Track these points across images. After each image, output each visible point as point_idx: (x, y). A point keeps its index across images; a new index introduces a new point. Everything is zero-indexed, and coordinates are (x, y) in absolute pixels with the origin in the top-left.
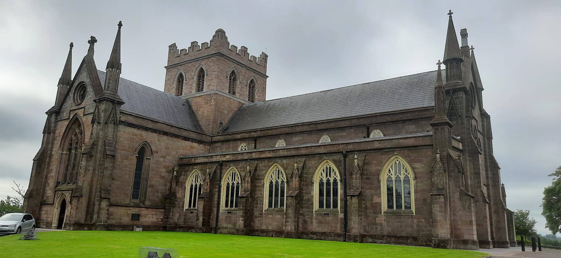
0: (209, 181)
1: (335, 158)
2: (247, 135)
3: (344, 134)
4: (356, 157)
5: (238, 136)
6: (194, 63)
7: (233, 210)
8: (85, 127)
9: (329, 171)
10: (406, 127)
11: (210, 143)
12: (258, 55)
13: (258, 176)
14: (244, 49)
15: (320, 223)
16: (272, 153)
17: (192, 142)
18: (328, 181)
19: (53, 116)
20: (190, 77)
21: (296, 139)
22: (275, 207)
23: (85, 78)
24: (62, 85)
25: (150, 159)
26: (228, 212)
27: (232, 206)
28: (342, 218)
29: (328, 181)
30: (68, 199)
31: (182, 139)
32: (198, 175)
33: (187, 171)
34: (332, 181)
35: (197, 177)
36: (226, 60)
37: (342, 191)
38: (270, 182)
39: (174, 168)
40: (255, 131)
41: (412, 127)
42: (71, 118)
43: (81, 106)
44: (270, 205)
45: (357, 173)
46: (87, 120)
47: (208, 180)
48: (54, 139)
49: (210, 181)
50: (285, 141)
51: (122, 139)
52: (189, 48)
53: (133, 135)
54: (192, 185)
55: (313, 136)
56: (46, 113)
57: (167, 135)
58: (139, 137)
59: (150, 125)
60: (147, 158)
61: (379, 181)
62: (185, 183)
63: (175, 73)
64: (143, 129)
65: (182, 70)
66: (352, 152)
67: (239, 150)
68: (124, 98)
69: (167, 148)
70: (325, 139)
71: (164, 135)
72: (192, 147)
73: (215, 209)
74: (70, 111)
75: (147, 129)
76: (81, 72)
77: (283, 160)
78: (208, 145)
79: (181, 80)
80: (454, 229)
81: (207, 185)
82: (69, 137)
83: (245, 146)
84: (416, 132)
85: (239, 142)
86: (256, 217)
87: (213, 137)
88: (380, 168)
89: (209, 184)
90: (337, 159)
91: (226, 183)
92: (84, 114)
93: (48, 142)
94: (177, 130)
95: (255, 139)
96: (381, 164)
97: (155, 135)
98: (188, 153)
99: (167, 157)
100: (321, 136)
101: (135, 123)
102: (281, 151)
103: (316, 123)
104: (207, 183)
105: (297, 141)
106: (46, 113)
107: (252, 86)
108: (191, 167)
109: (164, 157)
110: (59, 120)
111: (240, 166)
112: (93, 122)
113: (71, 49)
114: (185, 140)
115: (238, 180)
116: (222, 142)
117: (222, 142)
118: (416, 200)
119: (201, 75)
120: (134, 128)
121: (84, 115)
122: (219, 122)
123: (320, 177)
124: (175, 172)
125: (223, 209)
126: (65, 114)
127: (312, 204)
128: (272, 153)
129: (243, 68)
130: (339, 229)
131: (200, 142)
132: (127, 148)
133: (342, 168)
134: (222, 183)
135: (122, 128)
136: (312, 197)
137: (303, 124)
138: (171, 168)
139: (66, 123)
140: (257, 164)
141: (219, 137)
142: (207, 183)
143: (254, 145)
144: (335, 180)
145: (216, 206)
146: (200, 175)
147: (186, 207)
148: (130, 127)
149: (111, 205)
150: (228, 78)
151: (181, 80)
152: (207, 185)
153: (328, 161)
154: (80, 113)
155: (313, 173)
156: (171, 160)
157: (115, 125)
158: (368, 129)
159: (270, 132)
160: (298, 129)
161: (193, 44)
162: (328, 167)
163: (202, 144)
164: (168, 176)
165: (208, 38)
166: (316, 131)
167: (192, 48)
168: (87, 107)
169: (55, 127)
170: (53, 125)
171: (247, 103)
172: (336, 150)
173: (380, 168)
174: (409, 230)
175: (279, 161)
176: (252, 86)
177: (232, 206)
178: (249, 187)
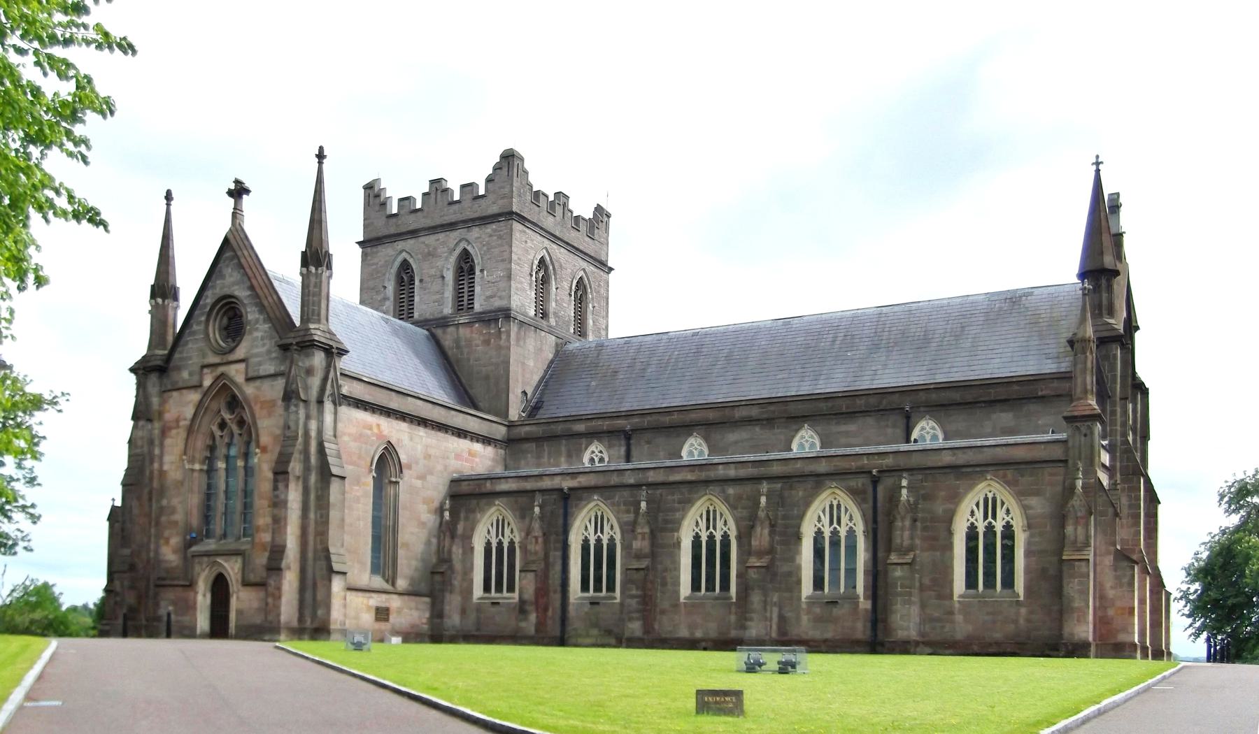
0: (541, 534)
1: (853, 483)
2: (605, 425)
3: (851, 427)
5: (580, 427)
6: (441, 236)
7: (605, 598)
8: (257, 408)
9: (834, 514)
10: (994, 416)
11: (505, 443)
12: (589, 214)
13: (666, 521)
15: (818, 620)
16: (697, 472)
17: (472, 440)
20: (433, 272)
22: (707, 589)
23: (231, 283)
24: (159, 300)
25: (399, 483)
26: (592, 603)
27: (598, 588)
28: (866, 610)
31: (453, 434)
32: (503, 520)
33: (473, 511)
34: (718, 538)
35: (500, 525)
36: (528, 231)
37: (869, 555)
38: (583, 541)
40: (629, 415)
41: (1005, 417)
43: (232, 357)
44: (696, 586)
45: (903, 519)
47: (537, 531)
49: (544, 534)
50: (707, 439)
51: (346, 438)
52: (424, 194)
53: (365, 427)
54: (489, 544)
55: (776, 431)
57: (426, 426)
58: (375, 430)
59: (395, 403)
60: (391, 482)
61: (950, 533)
64: (381, 414)
66: (896, 471)
68: (346, 341)
69: (428, 456)
70: (806, 442)
71: (419, 425)
72: (471, 453)
74: (203, 367)
75: (388, 412)
76: (220, 272)
77: (726, 487)
78: (501, 448)
79: (405, 277)
80: (1102, 622)
81: (537, 542)
82: (204, 429)
83: (601, 452)
85: (584, 441)
86: (663, 612)
87: (512, 428)
88: (952, 506)
89: (540, 540)
90: (857, 485)
91: (581, 538)
92: (247, 373)
94: (442, 411)
95: (627, 437)
96: (955, 498)
97: (404, 426)
99: (429, 478)
100: (797, 431)
101: (367, 398)
102: (721, 467)
103: (783, 401)
104: (536, 538)
105: (736, 442)
107: (581, 292)
108: (484, 501)
109: (422, 477)
110: (169, 387)
111: (617, 499)
113: (168, 205)
114: (459, 436)
115: (612, 531)
116: (538, 440)
117: (538, 440)
118: (1027, 571)
119: (465, 268)
120: (366, 410)
121: (248, 379)
122: (520, 391)
123: (816, 526)
125: (576, 597)
127: (799, 582)
128: (697, 472)
129: (562, 250)
131: (486, 440)
132: (355, 458)
135: (345, 411)
136: (799, 568)
137: (751, 403)
138: (436, 504)
140: (661, 495)
141: (527, 428)
142: (536, 538)
143: (623, 450)
145: (559, 589)
147: (478, 591)
148: (358, 407)
150: (534, 279)
151: (405, 277)
152: (537, 542)
153: (838, 491)
154: (237, 373)
155: (801, 517)
156: (436, 489)
157: (334, 403)
158: (908, 418)
159: (666, 419)
160: (738, 414)
161: (435, 185)
162: (835, 503)
163: (490, 444)
165: (479, 173)
166: (783, 420)
167: (433, 196)
168: (253, 360)
172: (854, 467)
173: (952, 506)
174: (1011, 628)
175: (718, 489)
176: (581, 292)
177: (598, 588)
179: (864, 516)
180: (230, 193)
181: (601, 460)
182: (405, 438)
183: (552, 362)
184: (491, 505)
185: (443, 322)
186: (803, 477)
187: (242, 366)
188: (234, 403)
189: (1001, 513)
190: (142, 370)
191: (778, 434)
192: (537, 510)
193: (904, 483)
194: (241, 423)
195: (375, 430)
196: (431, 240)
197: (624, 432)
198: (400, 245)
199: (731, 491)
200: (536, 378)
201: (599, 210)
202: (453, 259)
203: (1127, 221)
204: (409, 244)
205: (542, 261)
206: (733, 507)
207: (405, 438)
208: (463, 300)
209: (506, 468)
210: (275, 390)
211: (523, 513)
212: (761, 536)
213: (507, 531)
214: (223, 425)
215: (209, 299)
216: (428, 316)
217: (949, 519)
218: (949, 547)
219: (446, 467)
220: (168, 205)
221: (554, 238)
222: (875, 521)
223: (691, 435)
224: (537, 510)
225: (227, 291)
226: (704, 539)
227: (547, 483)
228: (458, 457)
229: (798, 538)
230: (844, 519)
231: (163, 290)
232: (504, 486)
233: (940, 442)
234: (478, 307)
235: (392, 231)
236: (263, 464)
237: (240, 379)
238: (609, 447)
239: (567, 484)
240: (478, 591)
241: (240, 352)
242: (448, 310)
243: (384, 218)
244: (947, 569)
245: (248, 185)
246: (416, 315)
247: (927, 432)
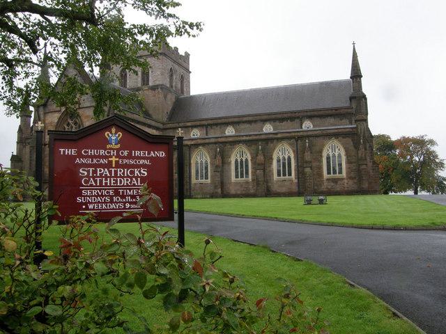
8: (83, 118)
14: (176, 49)
18: (242, 160)
21: (242, 126)
29: (242, 160)
84: (336, 125)
96: (323, 146)
127: (273, 174)
130: (295, 188)
133: (295, 149)
134: (192, 161)
139: (57, 115)
143: (205, 131)
144: (247, 160)
160: (245, 119)
169: (45, 117)
179: (294, 152)
183: (175, 103)
185: (138, 89)
186: (272, 140)
189: (337, 150)
191: (259, 124)
197: (205, 125)
200: (171, 108)
201: (186, 53)
203: (359, 59)
212: (261, 158)
217: (321, 152)
218: (321, 161)
221: (175, 62)
226: (239, 161)
229: (272, 159)
230: (287, 153)
233: (272, 131)
234: (151, 84)
242: (140, 85)
244: (320, 168)
246: (128, 87)
247: (308, 125)
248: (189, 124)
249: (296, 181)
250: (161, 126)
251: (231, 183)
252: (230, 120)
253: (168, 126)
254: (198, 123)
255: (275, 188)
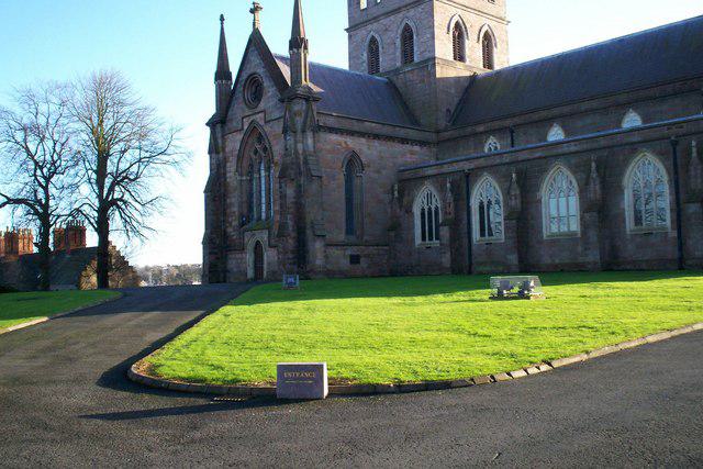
3: (665, 107)
4: (694, 143)
6: (392, 18)
19: (219, 126)
30: (265, 243)
35: (429, 196)
39: (393, 187)
42: (246, 127)
46: (273, 130)
48: (225, 160)
54: (423, 210)
56: (207, 124)
58: (344, 145)
62: (411, 206)
63: (364, 34)
65: (372, 30)
67: (486, 151)
72: (412, 153)
73: (466, 241)
93: (219, 166)
97: (363, 140)
98: (409, 159)
106: (207, 124)
109: (378, 172)
112: (285, 131)
113: (222, 24)
119: (407, 36)
122: (444, 110)
124: (396, 193)
126: (235, 124)
127: (624, 221)
130: (671, 251)
131: (422, 143)
139: (239, 137)
146: (434, 193)
149: (328, 245)
154: (259, 118)
164: (387, 198)
169: (223, 143)
170: (220, 141)
171: (480, 70)
178: (519, 205)
179: (667, 170)
180: (252, 11)
181: (496, 148)
182: (365, 149)
184: (422, 184)
185: (396, 71)
187: (261, 115)
188: (260, 139)
190: (212, 124)
192: (448, 185)
193: (694, 143)
194: (265, 149)
195: (344, 145)
196: (384, 21)
198: (369, 27)
199: (573, 161)
202: (400, 32)
204: (375, 26)
205: (457, 25)
206: (574, 173)
207: (365, 149)
208: (408, 54)
209: (437, 159)
210: (278, 127)
211: (442, 189)
213: (434, 201)
214: (256, 152)
215: (244, 76)
216: (388, 69)
219: (395, 164)
220: (222, 24)
222: (676, 173)
223: (552, 126)
224: (448, 185)
225: (252, 71)
227: (456, 167)
228: (404, 155)
231: (222, 73)
232: (430, 172)
235: (365, 19)
236: (275, 171)
237: (262, 123)
238: (500, 139)
239: (467, 166)
240: (418, 241)
241: (262, 105)
242: (399, 64)
243: (359, 13)
245: (261, 5)
248: (481, 129)
249: (675, 234)
250: (433, 137)
251: (541, 242)
252: (556, 111)
253: (446, 135)
254: (497, 124)
255: (629, 251)
